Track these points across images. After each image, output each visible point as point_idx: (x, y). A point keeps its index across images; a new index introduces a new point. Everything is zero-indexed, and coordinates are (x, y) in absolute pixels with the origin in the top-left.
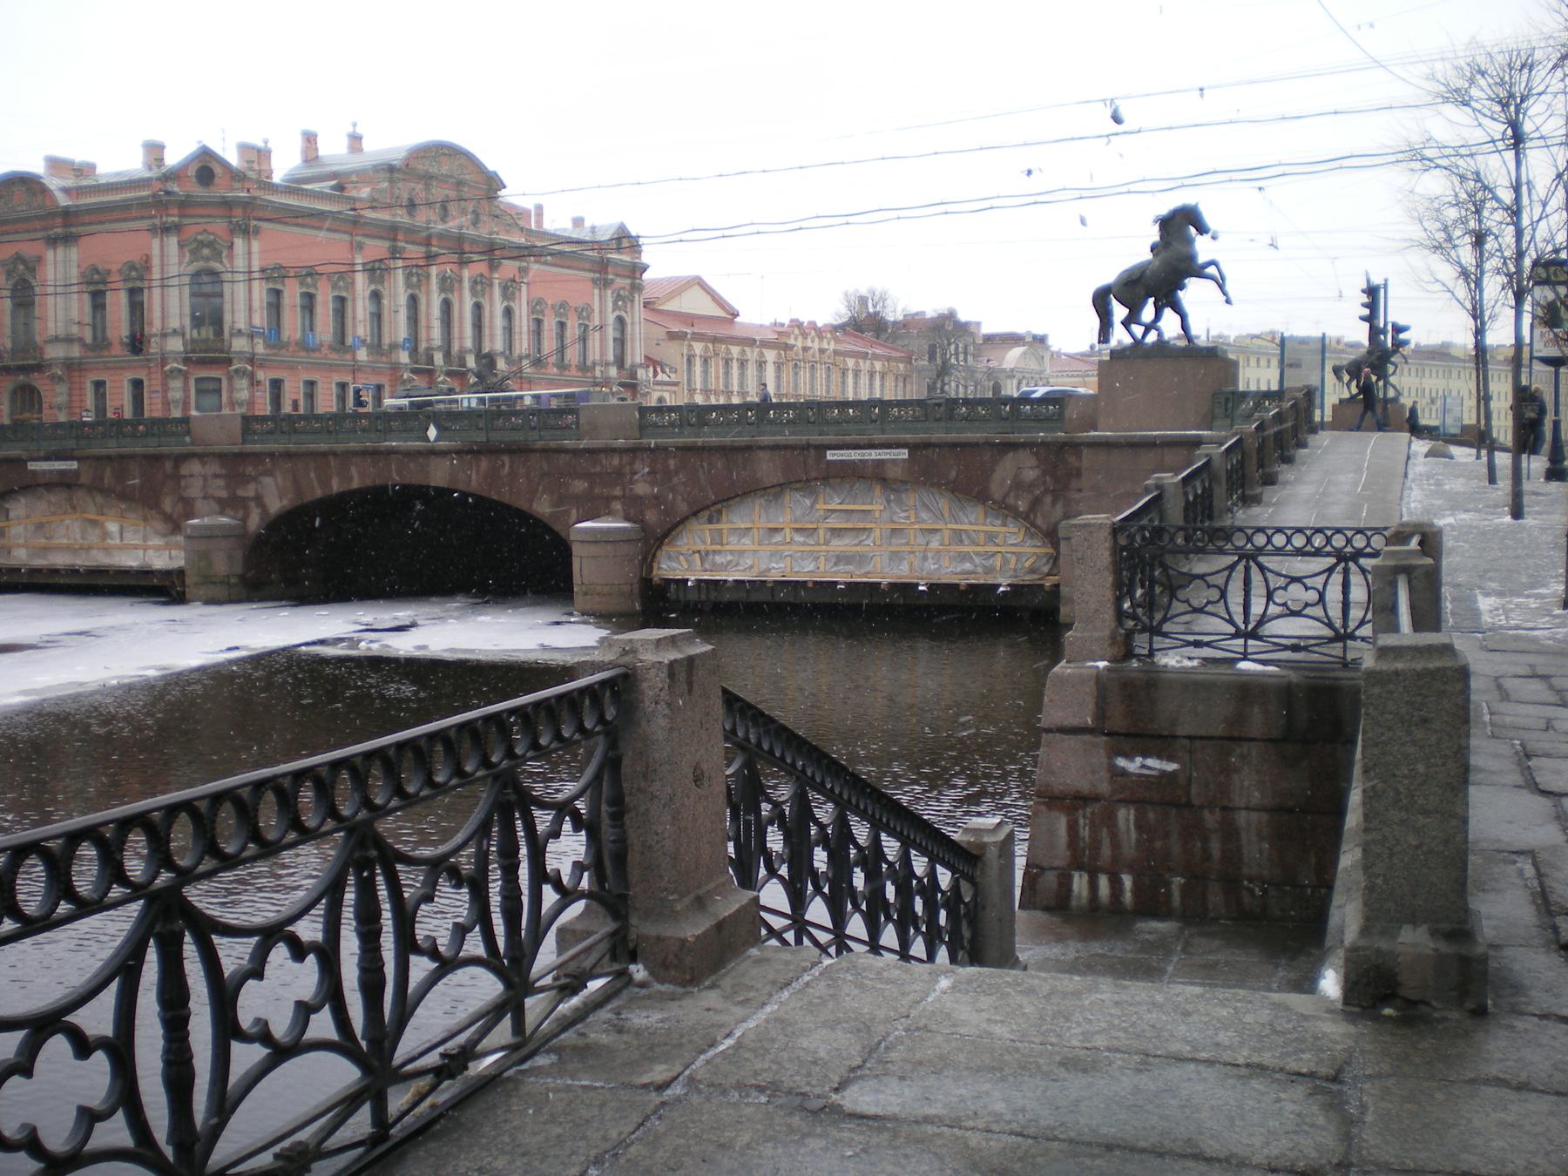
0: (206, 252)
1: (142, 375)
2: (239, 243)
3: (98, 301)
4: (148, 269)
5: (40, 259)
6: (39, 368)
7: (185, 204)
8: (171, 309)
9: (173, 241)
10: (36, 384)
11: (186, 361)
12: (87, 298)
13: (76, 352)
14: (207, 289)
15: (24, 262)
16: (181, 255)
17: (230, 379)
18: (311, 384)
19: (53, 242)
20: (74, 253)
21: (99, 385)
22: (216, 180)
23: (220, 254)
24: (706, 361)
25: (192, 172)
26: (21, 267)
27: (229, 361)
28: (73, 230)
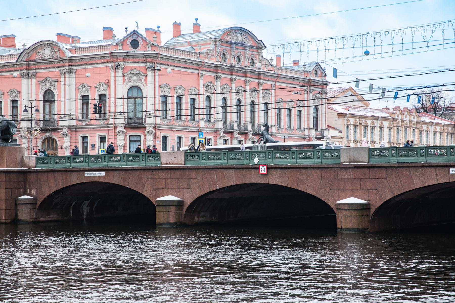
0: (135, 78)
2: (150, 73)
6: (55, 130)
7: (125, 57)
8: (118, 105)
9: (120, 73)
10: (54, 137)
13: (74, 123)
14: (135, 95)
17: (145, 136)
18: (180, 138)
21: (84, 138)
22: (140, 46)
23: (141, 80)
24: (355, 127)
25: (129, 42)
27: (145, 128)
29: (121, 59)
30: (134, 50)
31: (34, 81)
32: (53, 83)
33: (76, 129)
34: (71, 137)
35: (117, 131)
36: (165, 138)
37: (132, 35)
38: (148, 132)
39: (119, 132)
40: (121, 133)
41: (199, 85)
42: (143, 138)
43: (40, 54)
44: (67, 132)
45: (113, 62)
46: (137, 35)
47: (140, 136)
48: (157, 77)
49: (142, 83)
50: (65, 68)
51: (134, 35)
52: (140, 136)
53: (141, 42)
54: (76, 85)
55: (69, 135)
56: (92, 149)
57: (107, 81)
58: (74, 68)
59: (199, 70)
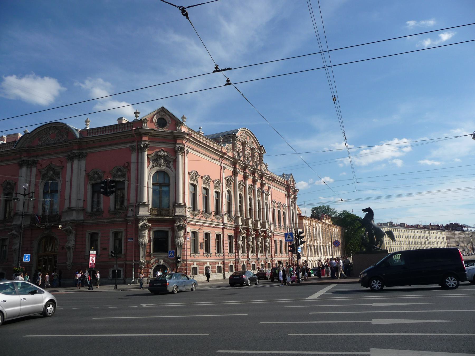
1: (122, 229)
4: (129, 170)
5: (64, 168)
11: (150, 221)
12: (89, 187)
14: (161, 181)
15: (54, 170)
16: (149, 162)
19: (71, 159)
20: (83, 163)
22: (168, 125)
25: (155, 120)
26: (51, 173)
27: (174, 221)
28: (84, 151)
29: (145, 138)
30: (161, 130)
31: (34, 170)
34: (76, 235)
35: (140, 225)
36: (195, 233)
38: (178, 226)
42: (170, 234)
43: (43, 139)
44: (71, 228)
46: (165, 112)
47: (166, 232)
48: (186, 163)
49: (170, 168)
52: (166, 232)
54: (86, 171)
55: (74, 232)
57: (126, 165)
58: (84, 151)
59: (221, 163)
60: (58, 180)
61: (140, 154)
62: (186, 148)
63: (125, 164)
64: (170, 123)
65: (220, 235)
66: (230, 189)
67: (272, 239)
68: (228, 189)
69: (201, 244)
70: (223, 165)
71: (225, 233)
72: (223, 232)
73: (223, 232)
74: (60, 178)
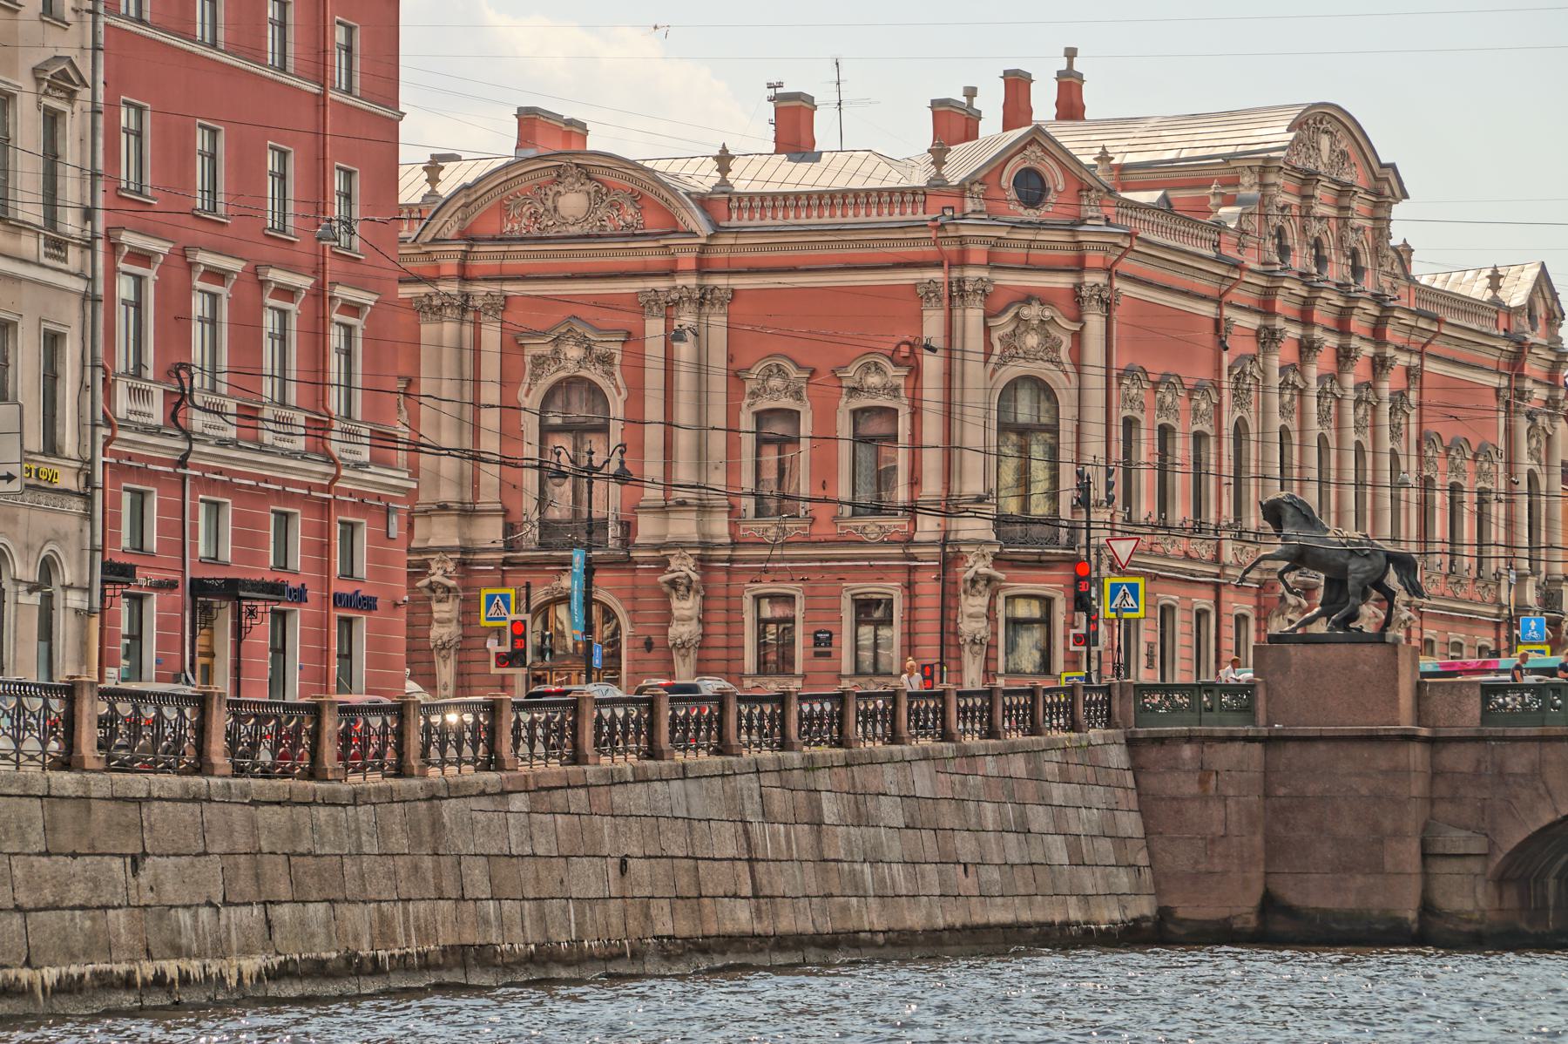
3: (776, 431)
22: (1052, 197)
23: (1056, 348)
32: (599, 349)
33: (731, 560)
37: (1024, 148)
39: (974, 582)
40: (980, 586)
41: (1219, 370)
45: (939, 265)
46: (1044, 149)
49: (1058, 363)
50: (680, 282)
51: (1030, 149)
53: (1056, 179)
56: (817, 654)
60: (610, 392)
61: (958, 313)
62: (1117, 284)
63: (897, 349)
64: (1060, 188)
65: (1207, 612)
66: (1246, 415)
67: (1415, 633)
68: (1238, 414)
69: (1150, 646)
70: (1227, 312)
71: (1225, 608)
72: (1218, 603)
73: (1218, 603)
74: (618, 375)
